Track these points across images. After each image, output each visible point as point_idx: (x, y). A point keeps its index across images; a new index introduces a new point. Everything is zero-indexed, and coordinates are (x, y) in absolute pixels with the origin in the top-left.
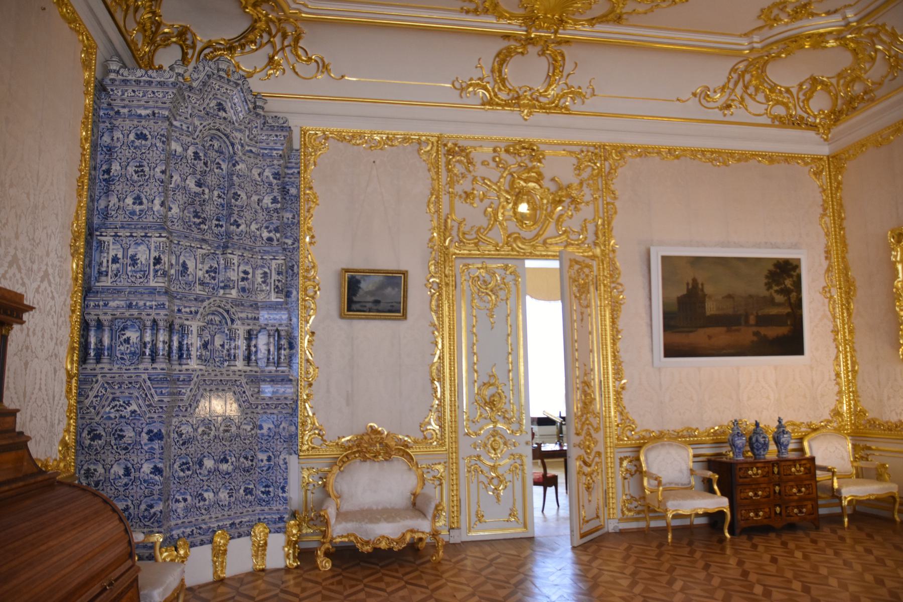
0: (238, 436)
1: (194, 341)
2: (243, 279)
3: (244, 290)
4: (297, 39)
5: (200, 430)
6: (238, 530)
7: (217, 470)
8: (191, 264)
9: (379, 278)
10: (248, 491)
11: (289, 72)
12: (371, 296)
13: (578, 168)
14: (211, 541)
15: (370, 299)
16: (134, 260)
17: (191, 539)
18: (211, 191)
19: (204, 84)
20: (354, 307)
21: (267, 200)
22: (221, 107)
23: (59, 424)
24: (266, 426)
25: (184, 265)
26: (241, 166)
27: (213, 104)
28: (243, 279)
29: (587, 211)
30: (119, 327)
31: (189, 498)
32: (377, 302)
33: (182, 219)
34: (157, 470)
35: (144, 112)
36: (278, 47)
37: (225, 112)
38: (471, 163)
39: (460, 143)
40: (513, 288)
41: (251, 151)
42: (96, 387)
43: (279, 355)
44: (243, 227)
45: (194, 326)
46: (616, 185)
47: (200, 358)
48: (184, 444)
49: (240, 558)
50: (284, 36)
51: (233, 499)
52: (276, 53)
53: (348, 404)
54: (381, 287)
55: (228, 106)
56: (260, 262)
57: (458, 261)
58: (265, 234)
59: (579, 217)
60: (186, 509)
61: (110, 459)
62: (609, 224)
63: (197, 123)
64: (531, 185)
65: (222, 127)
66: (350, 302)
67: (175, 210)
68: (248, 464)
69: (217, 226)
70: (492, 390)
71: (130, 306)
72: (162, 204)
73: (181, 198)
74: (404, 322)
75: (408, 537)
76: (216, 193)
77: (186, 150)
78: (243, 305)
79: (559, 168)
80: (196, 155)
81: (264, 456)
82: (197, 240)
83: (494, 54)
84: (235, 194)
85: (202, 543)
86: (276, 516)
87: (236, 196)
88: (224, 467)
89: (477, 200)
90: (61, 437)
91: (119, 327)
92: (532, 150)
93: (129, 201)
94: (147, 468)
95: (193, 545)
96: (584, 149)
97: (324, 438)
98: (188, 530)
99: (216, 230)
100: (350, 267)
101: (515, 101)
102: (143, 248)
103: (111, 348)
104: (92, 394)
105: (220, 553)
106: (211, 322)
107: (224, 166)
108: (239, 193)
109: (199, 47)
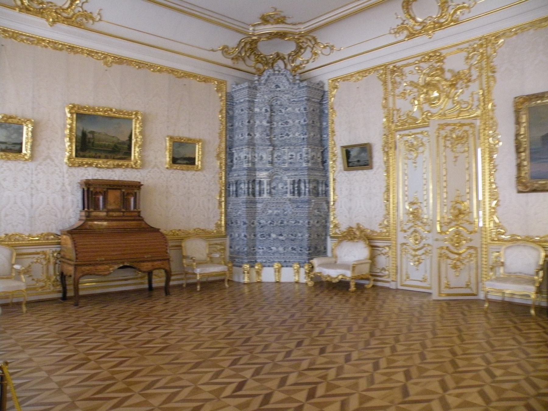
0: (288, 225)
1: (265, 187)
2: (291, 159)
3: (291, 163)
4: (314, 39)
5: (269, 222)
6: (286, 264)
7: (277, 239)
8: (264, 156)
9: (357, 149)
10: (293, 249)
11: (321, 55)
12: (358, 158)
13: (467, 58)
14: (273, 266)
15: (356, 160)
16: (240, 157)
17: (264, 264)
18: (277, 123)
19: (266, 80)
20: (350, 164)
21: (302, 121)
22: (277, 86)
23: (214, 217)
24: (301, 222)
25: (262, 157)
26: (289, 109)
27: (273, 86)
28: (291, 159)
29: (474, 87)
30: (237, 183)
31: (265, 248)
32: (359, 161)
33: (261, 138)
34: (245, 236)
35: (242, 101)
36: (312, 46)
37: (279, 87)
38: (402, 75)
39: (398, 64)
40: (427, 145)
41: (294, 101)
42: (230, 205)
43: (305, 190)
44: (291, 136)
45: (265, 181)
46: (496, 62)
47: (270, 193)
48: (262, 227)
49: (288, 275)
50: (310, 41)
51: (285, 251)
52: (312, 49)
53: (349, 212)
54: (360, 153)
55: (281, 86)
56: (299, 150)
57: (398, 133)
58: (302, 137)
59: (468, 92)
60: (264, 252)
61: (235, 230)
62: (489, 92)
63: (266, 97)
64: (437, 78)
65: (278, 95)
66: (348, 163)
67: (258, 135)
68: (293, 237)
69: (281, 137)
70: (415, 206)
71: (239, 176)
72: (249, 135)
73: (260, 130)
74: (370, 170)
75: (340, 277)
76: (280, 123)
77: (261, 110)
78: (289, 170)
79: (455, 63)
80: (266, 111)
81: (300, 235)
82: (266, 145)
83: (401, 7)
84: (287, 122)
85: (269, 266)
86: (303, 261)
87: (287, 123)
88: (281, 238)
89: (407, 96)
90: (217, 221)
91: (237, 183)
92: (436, 56)
93: (240, 136)
94: (243, 235)
95: (264, 266)
96: (472, 43)
97: (340, 229)
98: (264, 261)
99: (281, 139)
100: (345, 144)
101: (424, 29)
102: (242, 153)
103: (236, 191)
104: (229, 208)
105: (278, 271)
106: (276, 178)
107: (283, 111)
108: (289, 121)
109: (287, 57)
